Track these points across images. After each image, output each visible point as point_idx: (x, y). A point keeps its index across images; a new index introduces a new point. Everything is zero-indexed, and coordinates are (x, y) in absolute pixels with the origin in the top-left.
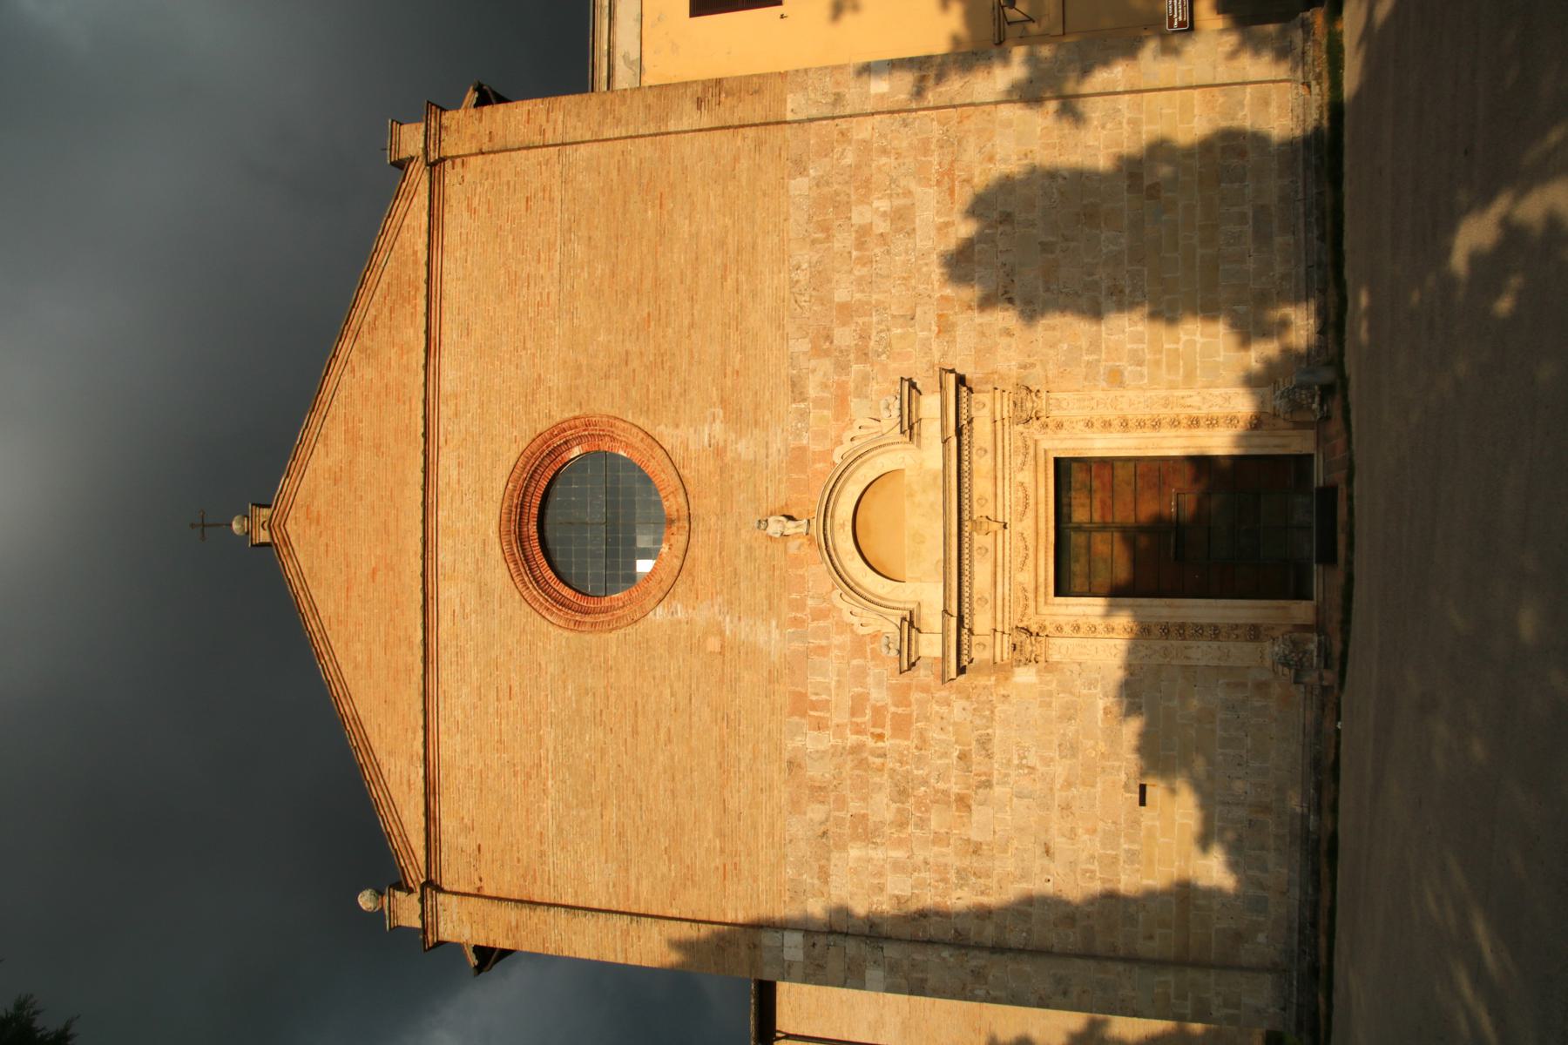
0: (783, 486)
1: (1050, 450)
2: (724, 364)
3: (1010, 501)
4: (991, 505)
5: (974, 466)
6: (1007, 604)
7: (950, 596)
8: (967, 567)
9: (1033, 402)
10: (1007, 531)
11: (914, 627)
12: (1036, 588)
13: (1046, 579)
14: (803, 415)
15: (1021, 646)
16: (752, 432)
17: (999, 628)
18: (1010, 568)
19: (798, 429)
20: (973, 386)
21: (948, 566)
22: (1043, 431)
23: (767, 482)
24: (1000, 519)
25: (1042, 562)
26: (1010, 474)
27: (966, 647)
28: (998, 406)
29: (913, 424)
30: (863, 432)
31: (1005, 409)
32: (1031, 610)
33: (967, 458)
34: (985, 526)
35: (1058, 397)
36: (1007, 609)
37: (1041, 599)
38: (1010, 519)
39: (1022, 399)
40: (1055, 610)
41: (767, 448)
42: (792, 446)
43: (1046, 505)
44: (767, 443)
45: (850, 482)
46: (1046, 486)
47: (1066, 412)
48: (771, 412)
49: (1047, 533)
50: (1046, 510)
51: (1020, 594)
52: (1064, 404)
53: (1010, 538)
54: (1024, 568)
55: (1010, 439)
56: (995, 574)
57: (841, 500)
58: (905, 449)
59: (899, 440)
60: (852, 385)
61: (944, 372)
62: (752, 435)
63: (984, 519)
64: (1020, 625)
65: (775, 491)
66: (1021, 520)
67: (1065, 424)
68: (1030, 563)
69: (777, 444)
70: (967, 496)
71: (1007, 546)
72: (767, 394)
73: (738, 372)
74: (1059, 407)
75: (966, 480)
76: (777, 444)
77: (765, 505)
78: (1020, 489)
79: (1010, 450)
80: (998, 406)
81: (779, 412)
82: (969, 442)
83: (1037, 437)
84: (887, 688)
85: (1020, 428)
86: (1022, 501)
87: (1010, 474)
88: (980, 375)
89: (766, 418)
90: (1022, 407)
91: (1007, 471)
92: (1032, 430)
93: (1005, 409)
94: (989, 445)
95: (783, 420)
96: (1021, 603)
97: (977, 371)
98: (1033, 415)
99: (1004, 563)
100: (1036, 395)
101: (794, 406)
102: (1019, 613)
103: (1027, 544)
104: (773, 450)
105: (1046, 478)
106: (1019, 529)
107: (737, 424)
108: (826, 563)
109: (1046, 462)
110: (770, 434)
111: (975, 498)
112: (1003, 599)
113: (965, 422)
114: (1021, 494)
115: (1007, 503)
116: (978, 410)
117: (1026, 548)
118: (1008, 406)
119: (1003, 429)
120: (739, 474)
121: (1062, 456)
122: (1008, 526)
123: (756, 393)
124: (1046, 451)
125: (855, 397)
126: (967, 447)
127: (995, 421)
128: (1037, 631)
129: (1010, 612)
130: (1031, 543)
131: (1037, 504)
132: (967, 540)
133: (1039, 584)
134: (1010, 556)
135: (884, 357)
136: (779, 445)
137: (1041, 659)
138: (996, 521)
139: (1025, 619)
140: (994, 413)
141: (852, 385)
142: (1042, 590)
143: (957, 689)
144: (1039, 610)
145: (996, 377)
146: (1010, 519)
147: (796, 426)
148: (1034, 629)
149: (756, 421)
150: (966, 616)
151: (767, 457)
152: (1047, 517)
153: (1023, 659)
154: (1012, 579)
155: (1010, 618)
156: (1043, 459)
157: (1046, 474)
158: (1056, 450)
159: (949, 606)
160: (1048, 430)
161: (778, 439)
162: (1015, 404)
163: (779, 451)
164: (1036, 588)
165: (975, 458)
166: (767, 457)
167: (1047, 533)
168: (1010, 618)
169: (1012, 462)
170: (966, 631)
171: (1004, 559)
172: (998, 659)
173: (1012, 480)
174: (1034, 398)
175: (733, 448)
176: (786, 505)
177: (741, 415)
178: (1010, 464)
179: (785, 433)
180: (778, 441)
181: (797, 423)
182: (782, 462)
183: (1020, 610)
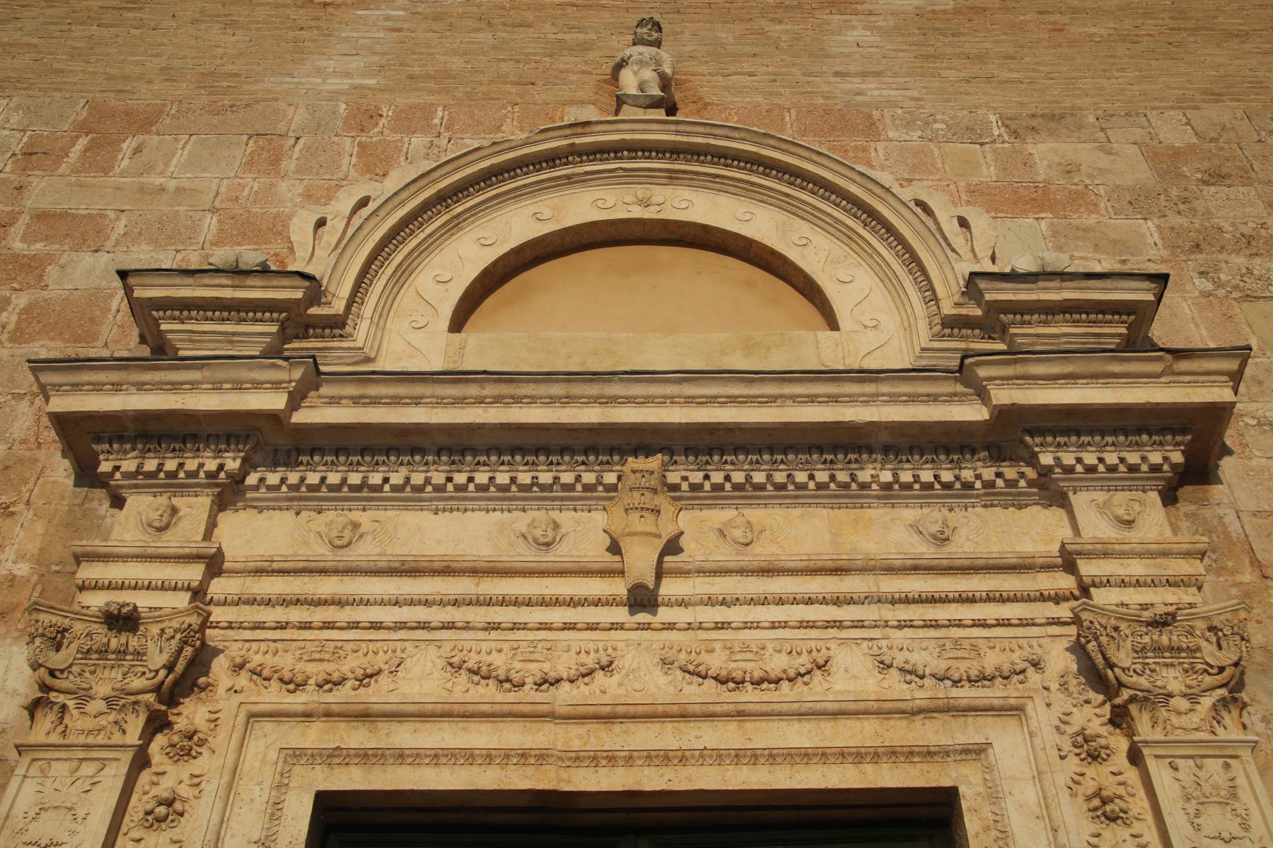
0: (759, 99)
1: (989, 768)
2: (1074, 11)
3: (747, 626)
4: (724, 554)
5: (877, 513)
6: (319, 615)
7: (375, 401)
8: (482, 478)
9: (1192, 698)
10: (621, 614)
11: (284, 335)
12: (365, 716)
13: (401, 756)
14: (975, 134)
15: (122, 653)
16: (903, 51)
17: (219, 587)
18: (467, 627)
19: (927, 123)
20: (1184, 507)
21: (490, 390)
22: (1067, 746)
23: (769, 74)
24: (669, 588)
25: (480, 736)
26: (858, 624)
27: (171, 465)
28: (1137, 568)
29: (1002, 331)
30: (951, 228)
31: (1135, 597)
32: (274, 697)
33: (906, 477)
34: (638, 523)
35: (1245, 794)
36: (296, 614)
37: (314, 736)
38: (670, 627)
39: (1193, 651)
40: (255, 792)
41: (864, 75)
42: (876, 114)
43: (739, 756)
44: (878, 74)
45: (780, 216)
46: (822, 755)
47: (1189, 831)
48: (968, 82)
49: (611, 759)
50: (718, 756)
51: (351, 664)
52: (1215, 820)
53: (591, 627)
54: (463, 677)
55: (1002, 623)
56: (447, 571)
57: (724, 200)
58: (909, 329)
59: (941, 291)
60: (1092, 220)
61: (1232, 365)
62: (894, 50)
63: (668, 531)
64: (219, 666)
65: (745, 87)
66: (664, 662)
67: (1121, 832)
68: (487, 693)
69: (873, 90)
70: (759, 477)
71: (558, 615)
72: (1014, 75)
73: (1061, 30)
74: (1197, 800)
75: (822, 476)
76: (873, 90)
77: (703, 69)
78: (803, 662)
79: (959, 624)
80: (1137, 568)
81: (968, 94)
82: (968, 486)
83: (1041, 717)
84: (98, 289)
85: (1060, 659)
86: (749, 666)
87: (858, 624)
88: (1234, 527)
89: (945, 73)
90: (1158, 649)
91: (868, 613)
92: (1061, 702)
93: (1135, 597)
94: (965, 545)
95: (948, 101)
96: (311, 668)
97: (1244, 517)
98: (1126, 694)
99: (489, 603)
100: (1223, 700)
101: (993, 118)
102: (269, 660)
103: (566, 686)
104: (855, 84)
105: (858, 756)
106: (627, 661)
107: (919, 29)
108: (526, 144)
109: (929, 754)
110: (902, 80)
111: (755, 514)
112: (339, 602)
113: (1046, 459)
114: (777, 664)
115: (736, 614)
116: (1103, 508)
117: (548, 682)
118: (1144, 607)
119: (1043, 598)
120: (787, 31)
121: (971, 824)
122: (643, 617)
123: (1012, 58)
124: (977, 752)
125: (1052, 224)
126: (947, 476)
127: (1069, 565)
128: (181, 724)
129: (281, 626)
130: (565, 696)
131: (741, 715)
132: (589, 478)
133: (383, 726)
134: (515, 627)
135: (1209, 286)
136: (876, 93)
137: (43, 730)
138: (660, 574)
139: (243, 680)
140: (1106, 555)
141: (1092, 220)
142: (357, 737)
143: (20, 461)
144: (268, 726)
145: (1248, 576)
146: (670, 627)
147: (936, 121)
148: (192, 713)
149: (933, 56)
150: (293, 478)
151: (837, 74)
152: (683, 758)
153: (58, 659)
154: (420, 634)
155: (258, 626)
156: (945, 740)
157: (876, 756)
158: (994, 795)
159: (334, 401)
160: (1073, 764)
161: (893, 93)
162: (1163, 622)
163: (858, 94)
164: (365, 716)
165: (910, 514)
166: (837, 74)
167: (611, 759)
168: (258, 626)
169: (908, 632)
170: (233, 464)
171: (504, 602)
172: (90, 572)
173: (833, 632)
174: (1207, 702)
175: (855, 23)
176: (706, 104)
177: (945, 36)
178: (901, 625)
179: (912, 103)
180: (885, 93)
181: (943, 122)
182: (826, 98)
183: (286, 662)
